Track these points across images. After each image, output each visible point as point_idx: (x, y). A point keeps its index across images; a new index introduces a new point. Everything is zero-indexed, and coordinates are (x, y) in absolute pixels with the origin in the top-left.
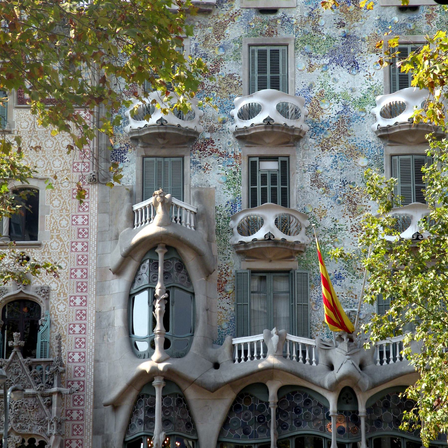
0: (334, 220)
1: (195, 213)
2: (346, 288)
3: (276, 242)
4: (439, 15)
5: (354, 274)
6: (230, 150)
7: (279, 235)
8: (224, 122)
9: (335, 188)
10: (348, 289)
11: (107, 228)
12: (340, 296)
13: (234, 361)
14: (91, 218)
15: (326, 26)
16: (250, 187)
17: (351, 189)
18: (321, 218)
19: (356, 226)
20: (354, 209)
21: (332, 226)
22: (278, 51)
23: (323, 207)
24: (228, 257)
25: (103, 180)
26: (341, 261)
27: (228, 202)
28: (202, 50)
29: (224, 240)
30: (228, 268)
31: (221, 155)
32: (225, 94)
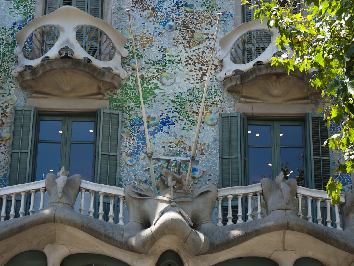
0: (163, 50)
2: (175, 135)
3: (77, 62)
5: (188, 119)
7: (80, 53)
9: (165, 11)
10: (179, 138)
12: (167, 147)
17: (187, 12)
18: (144, 47)
19: (193, 58)
20: (192, 38)
21: (160, 57)
23: (148, 33)
24: (8, 92)
26: (170, 102)
27: (15, 24)
29: (4, 70)
30: (7, 107)
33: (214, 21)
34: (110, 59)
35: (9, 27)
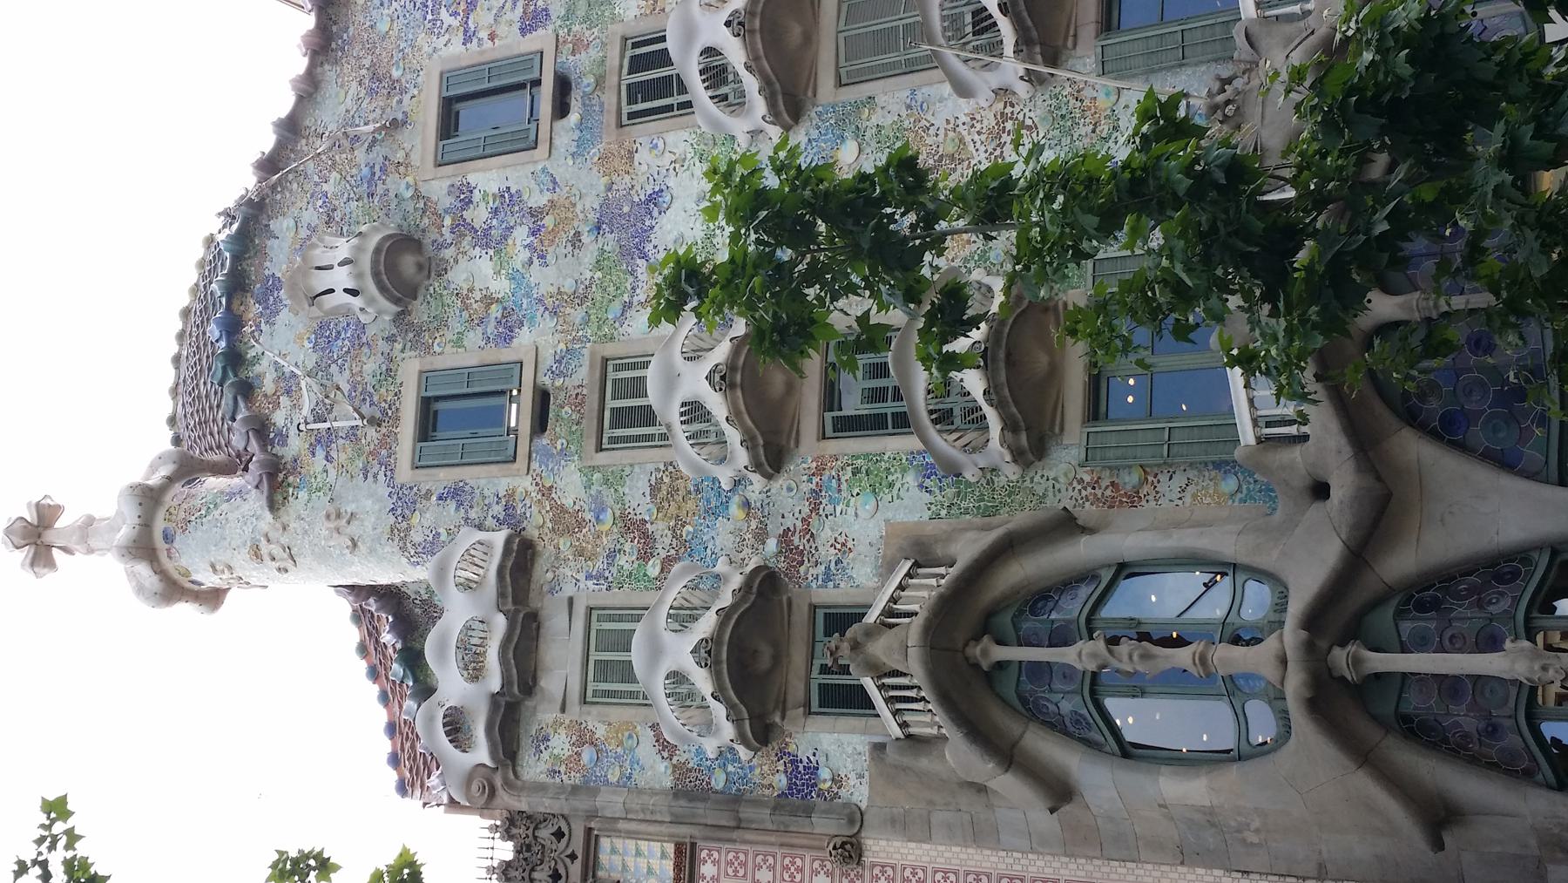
1: (917, 565)
4: (576, 28)
6: (806, 487)
8: (747, 504)
11: (967, 817)
13: (1304, 438)
14: (941, 863)
15: (576, 276)
16: (890, 430)
22: (614, 381)
25: (851, 822)
27: (921, 486)
28: (600, 564)
30: (1081, 481)
31: (815, 508)
32: (690, 505)
33: (924, 123)
34: (990, 289)
35: (927, 497)
